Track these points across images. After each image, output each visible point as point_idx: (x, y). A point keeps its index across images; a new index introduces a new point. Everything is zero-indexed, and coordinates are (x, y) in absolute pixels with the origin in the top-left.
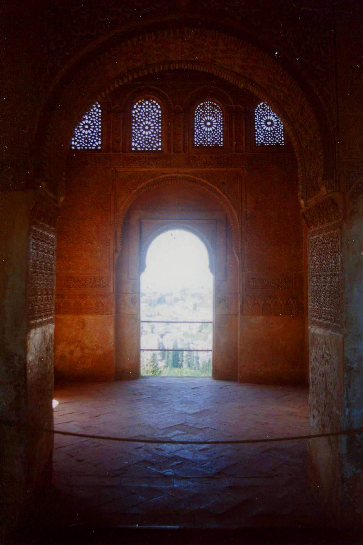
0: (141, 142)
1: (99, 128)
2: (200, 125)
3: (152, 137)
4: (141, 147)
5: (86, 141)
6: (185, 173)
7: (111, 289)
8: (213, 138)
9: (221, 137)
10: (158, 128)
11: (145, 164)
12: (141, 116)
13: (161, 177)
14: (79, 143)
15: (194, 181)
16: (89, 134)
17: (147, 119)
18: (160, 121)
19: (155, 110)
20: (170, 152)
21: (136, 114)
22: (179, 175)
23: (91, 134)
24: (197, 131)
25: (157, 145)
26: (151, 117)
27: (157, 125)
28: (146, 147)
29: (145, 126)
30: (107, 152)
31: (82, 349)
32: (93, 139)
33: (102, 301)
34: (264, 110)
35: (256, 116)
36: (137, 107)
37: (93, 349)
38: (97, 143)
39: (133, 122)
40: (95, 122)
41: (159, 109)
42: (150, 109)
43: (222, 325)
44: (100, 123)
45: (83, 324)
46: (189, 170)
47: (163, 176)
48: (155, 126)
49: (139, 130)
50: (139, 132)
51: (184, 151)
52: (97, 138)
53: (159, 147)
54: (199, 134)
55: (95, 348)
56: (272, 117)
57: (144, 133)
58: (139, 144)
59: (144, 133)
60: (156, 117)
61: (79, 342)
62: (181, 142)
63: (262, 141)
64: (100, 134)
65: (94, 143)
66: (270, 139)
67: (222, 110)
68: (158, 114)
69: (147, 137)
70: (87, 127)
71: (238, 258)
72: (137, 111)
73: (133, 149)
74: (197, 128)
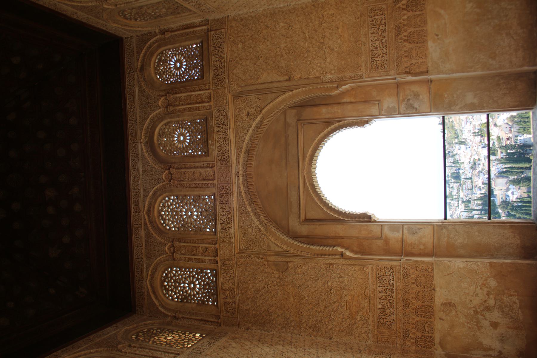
1: (193, 271)
7: (395, 263)
11: (230, 216)
13: (244, 196)
15: (249, 153)
16: (199, 284)
21: (174, 227)
22: (240, 172)
24: (190, 151)
26: (177, 208)
29: (188, 216)
30: (217, 262)
31: (488, 309)
32: (205, 279)
33: (413, 276)
34: (164, 73)
35: (171, 82)
37: (488, 294)
38: (210, 274)
41: (169, 199)
43: (442, 101)
45: (448, 305)
46: (234, 158)
47: (243, 192)
48: (186, 204)
51: (212, 167)
55: (486, 290)
56: (172, 63)
57: (195, 217)
61: (476, 312)
65: (209, 278)
68: (173, 200)
71: (344, 87)
74: (187, 151)
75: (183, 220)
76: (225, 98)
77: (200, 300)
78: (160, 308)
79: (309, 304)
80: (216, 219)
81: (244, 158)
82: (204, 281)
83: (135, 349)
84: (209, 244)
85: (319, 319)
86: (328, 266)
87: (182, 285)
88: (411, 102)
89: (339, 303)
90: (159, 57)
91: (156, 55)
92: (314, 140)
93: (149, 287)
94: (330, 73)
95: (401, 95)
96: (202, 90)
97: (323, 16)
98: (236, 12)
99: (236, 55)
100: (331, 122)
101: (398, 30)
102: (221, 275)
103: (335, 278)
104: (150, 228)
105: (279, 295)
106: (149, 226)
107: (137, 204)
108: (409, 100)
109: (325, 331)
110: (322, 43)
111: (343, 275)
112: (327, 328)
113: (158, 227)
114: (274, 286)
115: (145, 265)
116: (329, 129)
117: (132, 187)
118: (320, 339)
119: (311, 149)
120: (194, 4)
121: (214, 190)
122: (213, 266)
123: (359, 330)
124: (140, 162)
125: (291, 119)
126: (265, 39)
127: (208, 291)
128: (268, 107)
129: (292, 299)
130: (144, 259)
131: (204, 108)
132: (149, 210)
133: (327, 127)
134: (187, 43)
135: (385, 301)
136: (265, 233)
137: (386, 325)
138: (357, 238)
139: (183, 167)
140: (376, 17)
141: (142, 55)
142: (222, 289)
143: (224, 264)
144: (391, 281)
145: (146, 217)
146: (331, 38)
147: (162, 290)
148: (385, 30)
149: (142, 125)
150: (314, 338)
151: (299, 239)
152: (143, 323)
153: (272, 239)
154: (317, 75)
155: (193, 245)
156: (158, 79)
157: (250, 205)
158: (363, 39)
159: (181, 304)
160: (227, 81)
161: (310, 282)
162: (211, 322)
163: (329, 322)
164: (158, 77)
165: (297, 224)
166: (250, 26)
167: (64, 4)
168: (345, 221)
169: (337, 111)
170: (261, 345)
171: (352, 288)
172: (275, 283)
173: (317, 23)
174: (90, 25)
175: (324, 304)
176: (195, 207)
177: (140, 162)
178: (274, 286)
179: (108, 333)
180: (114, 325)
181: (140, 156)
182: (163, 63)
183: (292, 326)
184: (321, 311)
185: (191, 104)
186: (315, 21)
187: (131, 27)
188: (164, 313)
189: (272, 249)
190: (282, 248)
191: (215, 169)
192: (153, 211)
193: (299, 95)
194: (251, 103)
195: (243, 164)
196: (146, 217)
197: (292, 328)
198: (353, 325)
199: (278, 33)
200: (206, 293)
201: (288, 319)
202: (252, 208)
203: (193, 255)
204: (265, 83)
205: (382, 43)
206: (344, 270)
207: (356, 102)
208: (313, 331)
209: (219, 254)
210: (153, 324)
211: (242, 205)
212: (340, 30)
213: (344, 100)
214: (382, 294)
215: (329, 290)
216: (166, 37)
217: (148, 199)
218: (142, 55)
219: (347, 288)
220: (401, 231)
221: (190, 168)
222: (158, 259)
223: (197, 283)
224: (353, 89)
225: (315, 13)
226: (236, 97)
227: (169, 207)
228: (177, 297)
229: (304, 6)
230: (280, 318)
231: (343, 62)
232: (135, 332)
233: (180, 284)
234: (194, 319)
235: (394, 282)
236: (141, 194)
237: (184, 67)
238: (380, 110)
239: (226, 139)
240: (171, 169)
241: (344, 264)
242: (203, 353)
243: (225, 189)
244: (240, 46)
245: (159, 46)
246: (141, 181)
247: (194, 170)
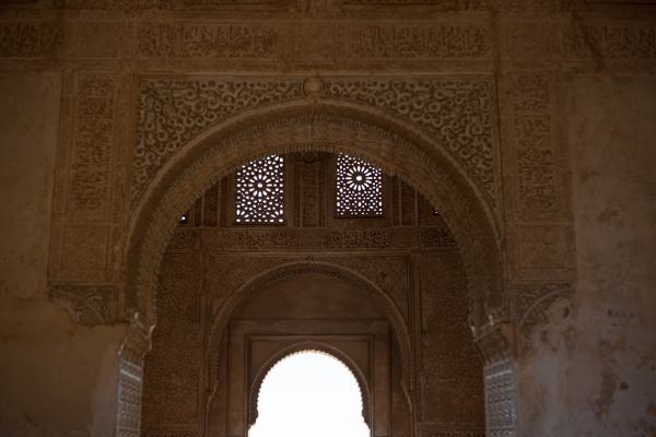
2: (345, 181)
3: (268, 201)
4: (251, 217)
6: (322, 259)
8: (367, 201)
9: (379, 201)
10: (278, 186)
13: (282, 266)
20: (299, 226)
26: (267, 168)
39: (239, 177)
46: (330, 253)
48: (273, 182)
49: (247, 189)
53: (281, 216)
57: (255, 194)
58: (248, 212)
60: (274, 168)
68: (278, 162)
74: (341, 186)
96: (419, 213)
116: (361, 373)
121: (290, 225)
128: (390, 301)
136: (236, 292)
143: (194, 234)
153: (228, 303)
154: (426, 367)
155: (220, 191)
168: (249, 393)
172: (172, 304)
178: (168, 303)
185: (403, 194)
190: (217, 314)
191: (318, 228)
207: (391, 410)
213: (394, 395)
221: (320, 192)
224: (407, 406)
240: (319, 163)
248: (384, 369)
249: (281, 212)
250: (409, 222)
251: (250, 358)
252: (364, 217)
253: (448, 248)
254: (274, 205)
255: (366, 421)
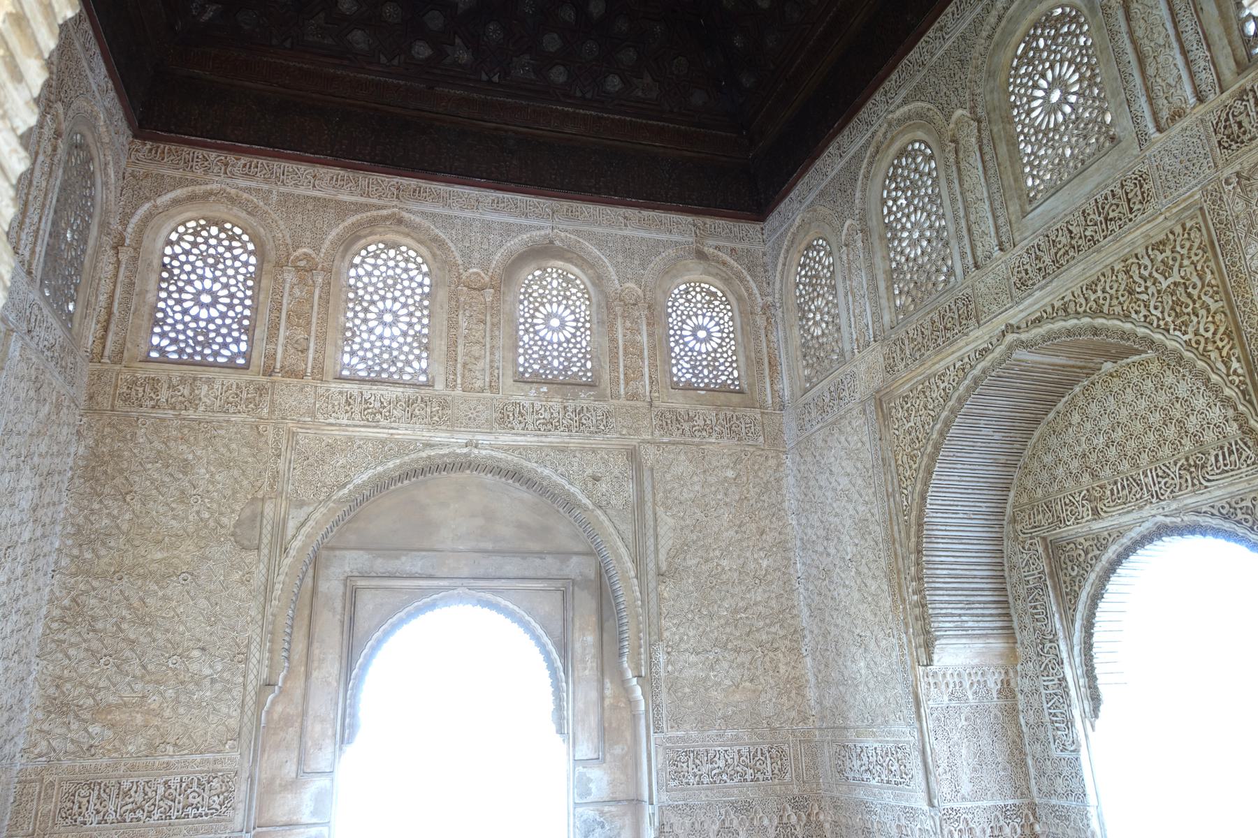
0: (369, 355)
1: (245, 307)
2: (533, 325)
3: (401, 346)
4: (369, 369)
5: (200, 338)
8: (566, 359)
11: (378, 416)
12: (374, 285)
13: (424, 454)
14: (175, 341)
16: (210, 320)
17: (389, 295)
18: (426, 303)
19: (412, 273)
21: (359, 278)
22: (476, 451)
23: (219, 321)
24: (526, 338)
25: (416, 364)
27: (418, 314)
28: (383, 370)
32: (224, 336)
34: (689, 301)
35: (670, 315)
36: (363, 262)
39: (351, 300)
40: (233, 289)
41: (425, 275)
42: (398, 271)
44: (249, 293)
46: (506, 439)
49: (365, 321)
50: (364, 328)
52: (235, 334)
54: (530, 347)
57: (378, 331)
58: (363, 359)
59: (378, 331)
62: (483, 364)
63: (688, 376)
64: (246, 322)
65: (225, 345)
66: (706, 372)
67: (588, 292)
68: (421, 285)
69: (387, 342)
70: (206, 299)
71: (638, 692)
72: (361, 272)
73: (346, 373)
74: (526, 331)
75: (373, 302)
76: (632, 431)
77: (166, 316)
78: (147, 206)
79: (142, 600)
80: (373, 382)
81: (507, 462)
82: (217, 331)
83: (49, 149)
84: (314, 359)
85: (99, 625)
86: (244, 650)
87: (209, 274)
88: (599, 830)
89: (143, 676)
90: (720, 294)
91: (725, 289)
92: (529, 614)
93: (209, 187)
94: (668, 662)
95: (613, 809)
96: (651, 383)
97: (776, 649)
98: (795, 472)
99: (715, 463)
100: (566, 651)
101: (744, 808)
102: (233, 378)
103: (211, 667)
104: (358, 217)
105: (173, 522)
106: (364, 215)
107: (416, 194)
108: (603, 827)
109: (64, 642)
110: (725, 645)
111: (218, 686)
112: (71, 645)
113: (359, 238)
114: (198, 512)
115: (266, 187)
116: (551, 647)
117: (458, 189)
118: (39, 629)
119: (511, 606)
120: (827, 400)
122: (258, 360)
123: (59, 731)
124: (512, 220)
125: (577, 567)
126: (740, 526)
127: (188, 337)
128: (607, 523)
129: (159, 556)
130: (282, 189)
131: (615, 381)
132: (400, 221)
133: (555, 644)
134: (742, 359)
135: (139, 798)
137: (69, 805)
138: (304, 714)
139: (495, 320)
140: (769, 761)
141: (728, 259)
142: (195, 379)
143: (261, 390)
144: (195, 811)
145: (385, 212)
146: (734, 665)
147: (197, 220)
148: (745, 780)
149: (591, 237)
150: (44, 611)
151: (311, 572)
152: (110, 158)
153: (317, 515)
154: (666, 634)
155: (314, 320)
156: (677, 287)
157: (401, 466)
158: (729, 733)
159: (156, 263)
160: (665, 440)
161: (203, 603)
162: (104, 338)
163: (87, 650)
164: (683, 287)
165: (348, 569)
166: (765, 498)
167: (869, 142)
168: (347, 684)
169: (587, 668)
170: (37, 480)
171: (181, 710)
172: (207, 515)
173: (764, 637)
174: (805, 170)
175: (142, 639)
176: (405, 334)
177: (512, 220)
178: (198, 512)
179: (92, 70)
180: (110, 85)
181: (523, 221)
182: (710, 302)
183: (81, 551)
184: (122, 631)
185: (625, 354)
186: (768, 633)
187: (787, 251)
188: (133, 214)
189: (293, 512)
191: (488, 394)
192: (398, 232)
193: (628, 591)
194: (617, 486)
195: (492, 457)
196: (385, 212)
197: (76, 552)
198: (77, 716)
199: (748, 554)
200: (184, 332)
201: (104, 544)
202: (394, 469)
203: (288, 317)
204: (656, 520)
205: (720, 774)
206: (229, 691)
208: (65, 608)
209: (288, 380)
210: (105, 184)
211: (402, 447)
212: (748, 684)
213: (608, 685)
214: (161, 790)
215: (180, 651)
216: (758, 318)
217: (426, 223)
218: (728, 259)
219: (183, 698)
220: (314, 820)
222: (281, 222)
223: (214, 313)
224: (631, 703)
225: (781, 633)
226: (633, 455)
227: (406, 270)
228: (175, 257)
229: (795, 612)
230: (106, 521)
231: (687, 690)
232: (90, 139)
233: (214, 266)
234: (114, 291)
235: (191, 819)
236: (439, 210)
237: (697, 348)
238: (585, 762)
239: (549, 427)
241: (245, 689)
242: (27, 338)
243: (441, 412)
244: (730, 474)
245: (740, 299)
246: (468, 214)
247: (488, 346)
248: (590, 638)
249: (424, 364)
250: (633, 397)
251: (352, 620)
252: (563, 384)
253: (697, 440)
254: (411, 352)
255: (560, 731)
